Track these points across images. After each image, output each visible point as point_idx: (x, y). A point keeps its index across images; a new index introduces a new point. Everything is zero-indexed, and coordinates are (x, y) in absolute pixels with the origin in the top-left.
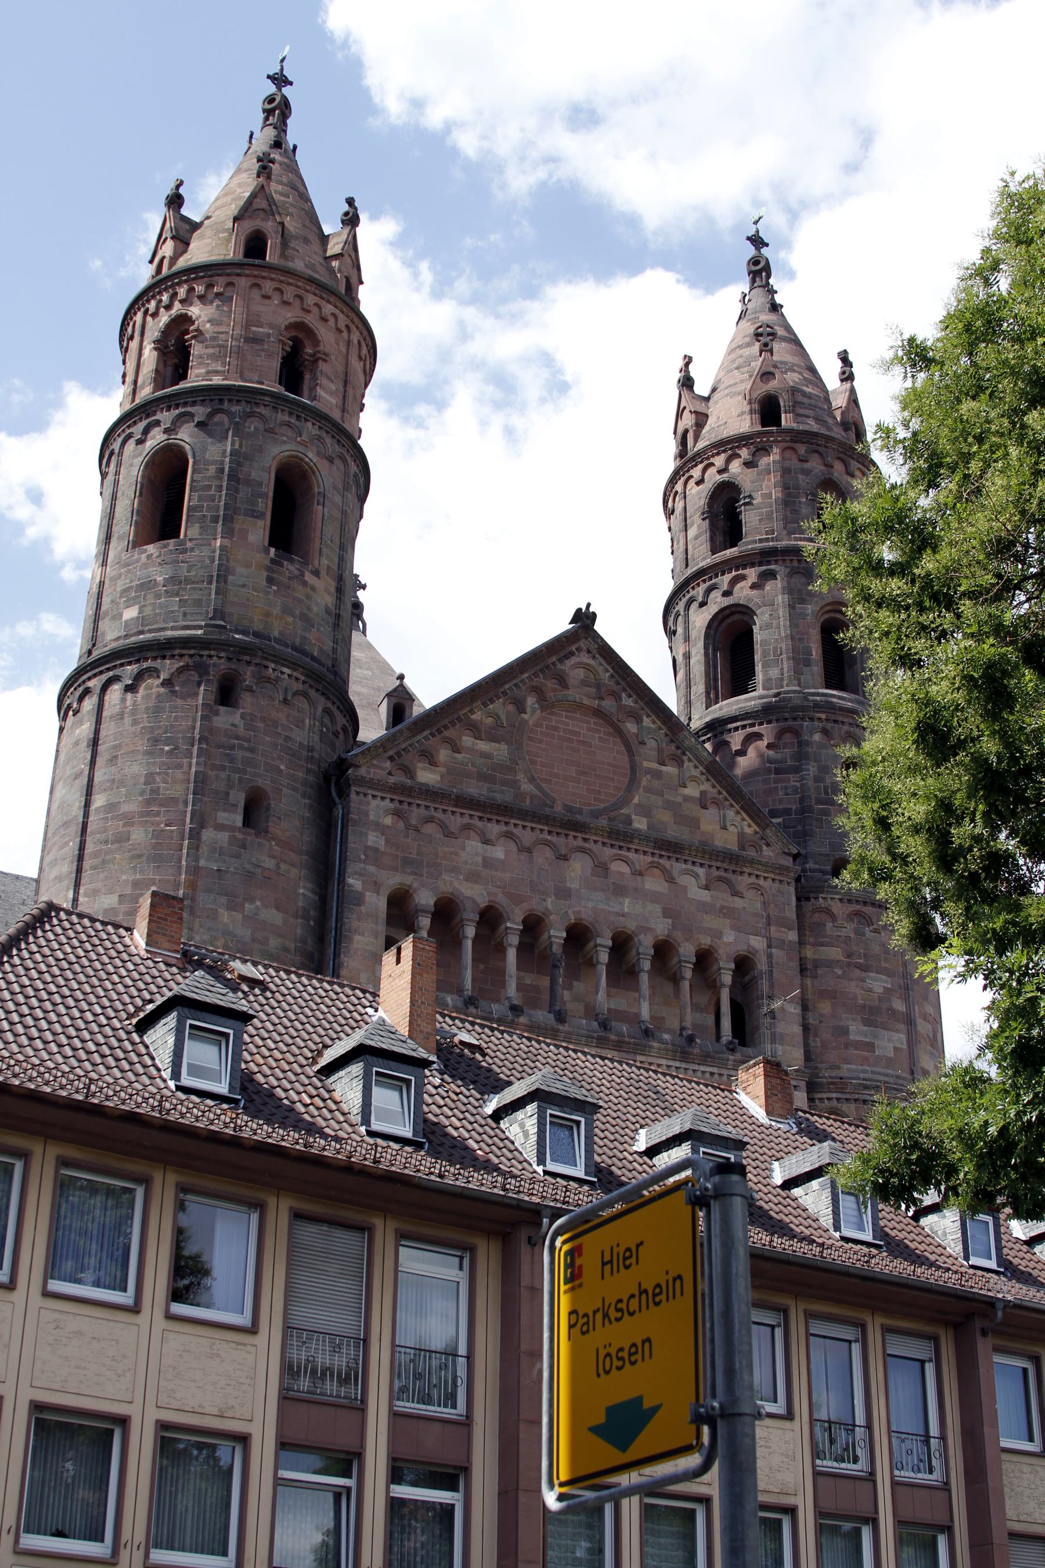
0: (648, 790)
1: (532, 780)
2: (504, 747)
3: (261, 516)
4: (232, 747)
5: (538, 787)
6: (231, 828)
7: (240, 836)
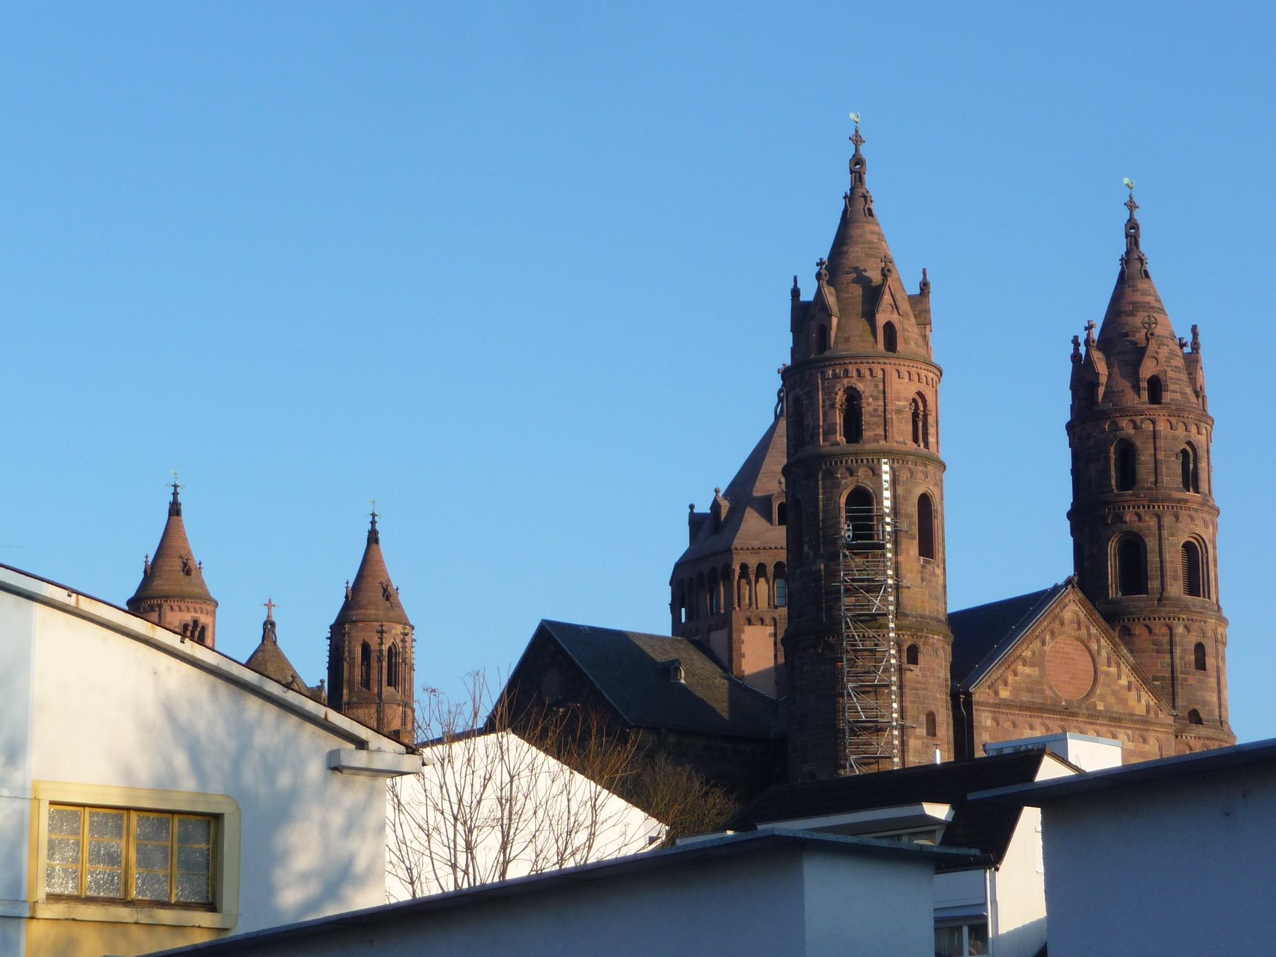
0: (1104, 685)
1: (1050, 688)
2: (1037, 669)
3: (913, 538)
4: (917, 689)
5: (1054, 692)
6: (922, 738)
7: (926, 741)
